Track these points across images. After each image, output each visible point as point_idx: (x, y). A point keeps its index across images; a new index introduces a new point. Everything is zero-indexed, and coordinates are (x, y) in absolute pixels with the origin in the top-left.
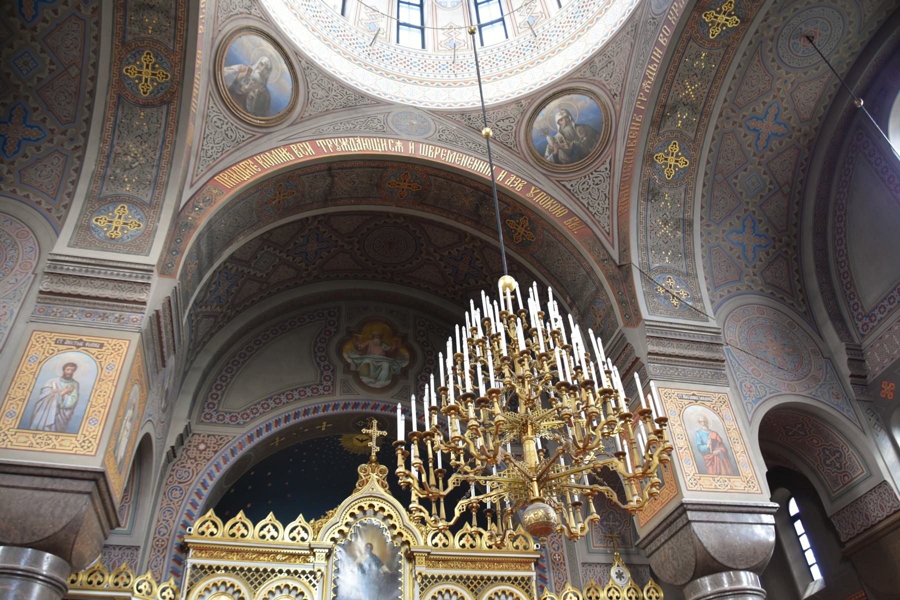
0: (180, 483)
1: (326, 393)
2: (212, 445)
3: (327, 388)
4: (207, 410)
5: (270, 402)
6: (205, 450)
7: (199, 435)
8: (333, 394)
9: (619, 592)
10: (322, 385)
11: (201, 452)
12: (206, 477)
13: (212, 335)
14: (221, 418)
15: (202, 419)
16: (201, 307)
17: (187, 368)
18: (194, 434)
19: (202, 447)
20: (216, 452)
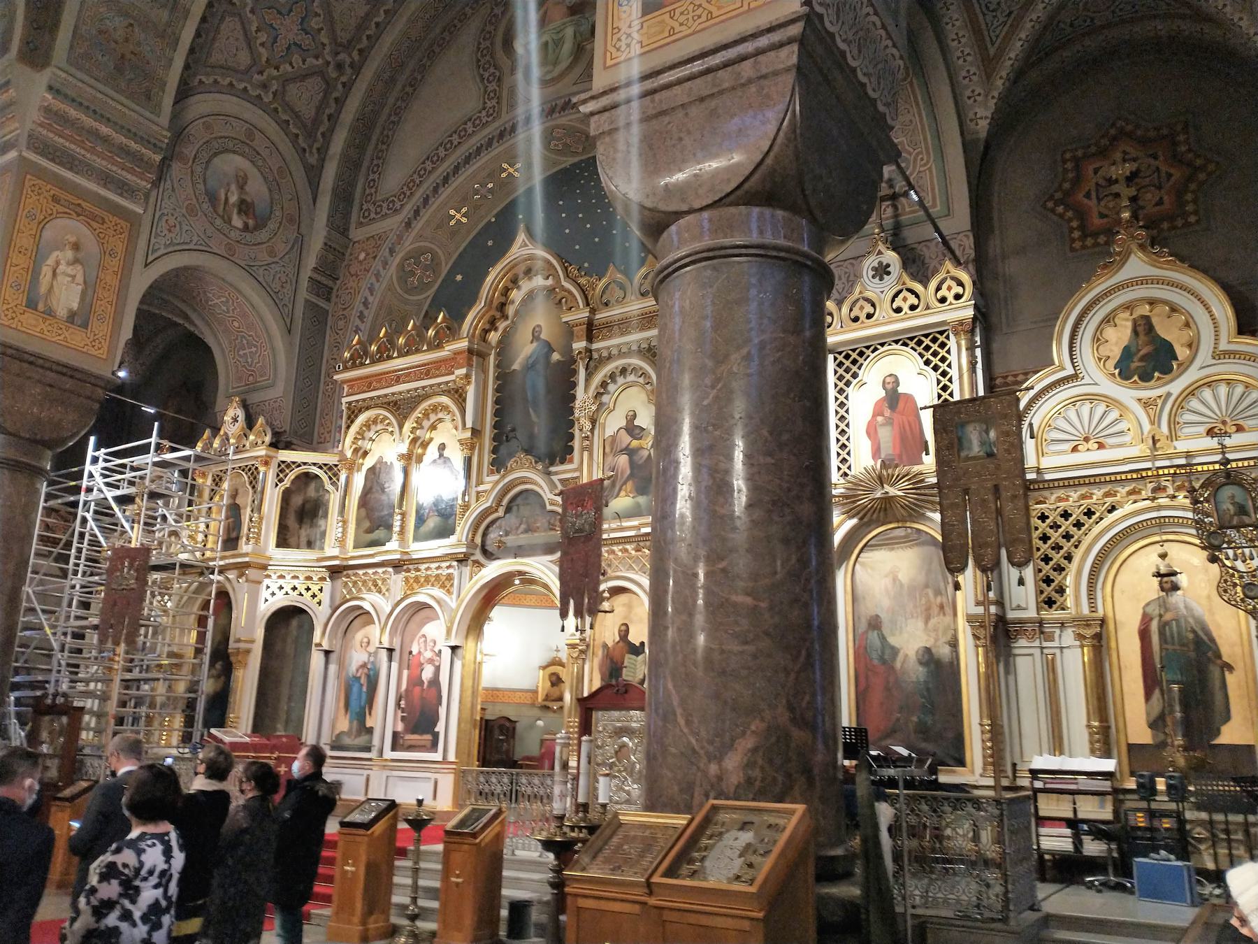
0: (345, 309)
1: (491, 118)
2: (371, 251)
3: (491, 111)
4: (365, 207)
5: (428, 163)
6: (365, 259)
7: (358, 242)
8: (499, 115)
9: (917, 296)
10: (484, 109)
11: (361, 262)
12: (367, 293)
13: (340, 102)
14: (378, 210)
15: (361, 219)
16: (261, 73)
17: (313, 160)
18: (354, 243)
19: (362, 256)
20: (375, 257)
